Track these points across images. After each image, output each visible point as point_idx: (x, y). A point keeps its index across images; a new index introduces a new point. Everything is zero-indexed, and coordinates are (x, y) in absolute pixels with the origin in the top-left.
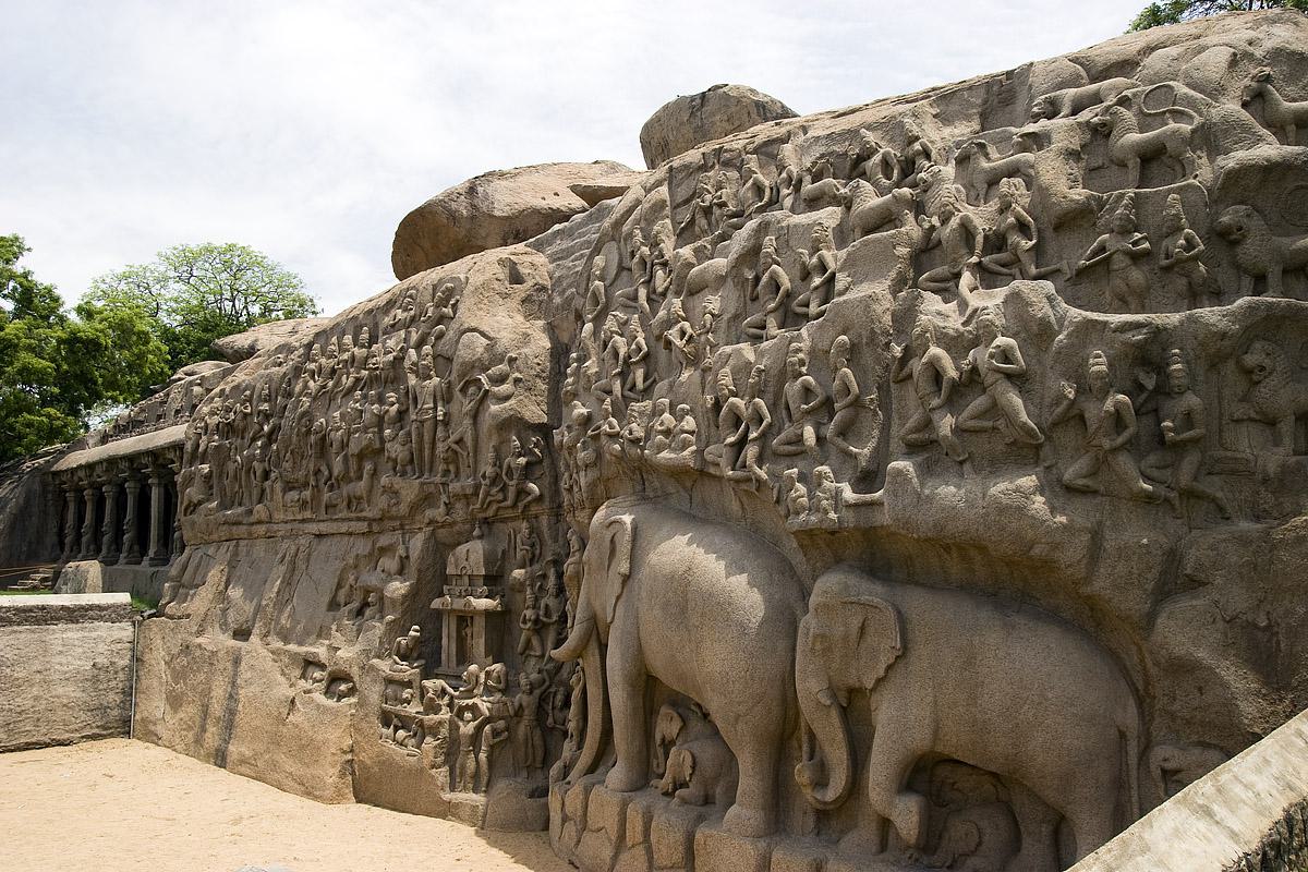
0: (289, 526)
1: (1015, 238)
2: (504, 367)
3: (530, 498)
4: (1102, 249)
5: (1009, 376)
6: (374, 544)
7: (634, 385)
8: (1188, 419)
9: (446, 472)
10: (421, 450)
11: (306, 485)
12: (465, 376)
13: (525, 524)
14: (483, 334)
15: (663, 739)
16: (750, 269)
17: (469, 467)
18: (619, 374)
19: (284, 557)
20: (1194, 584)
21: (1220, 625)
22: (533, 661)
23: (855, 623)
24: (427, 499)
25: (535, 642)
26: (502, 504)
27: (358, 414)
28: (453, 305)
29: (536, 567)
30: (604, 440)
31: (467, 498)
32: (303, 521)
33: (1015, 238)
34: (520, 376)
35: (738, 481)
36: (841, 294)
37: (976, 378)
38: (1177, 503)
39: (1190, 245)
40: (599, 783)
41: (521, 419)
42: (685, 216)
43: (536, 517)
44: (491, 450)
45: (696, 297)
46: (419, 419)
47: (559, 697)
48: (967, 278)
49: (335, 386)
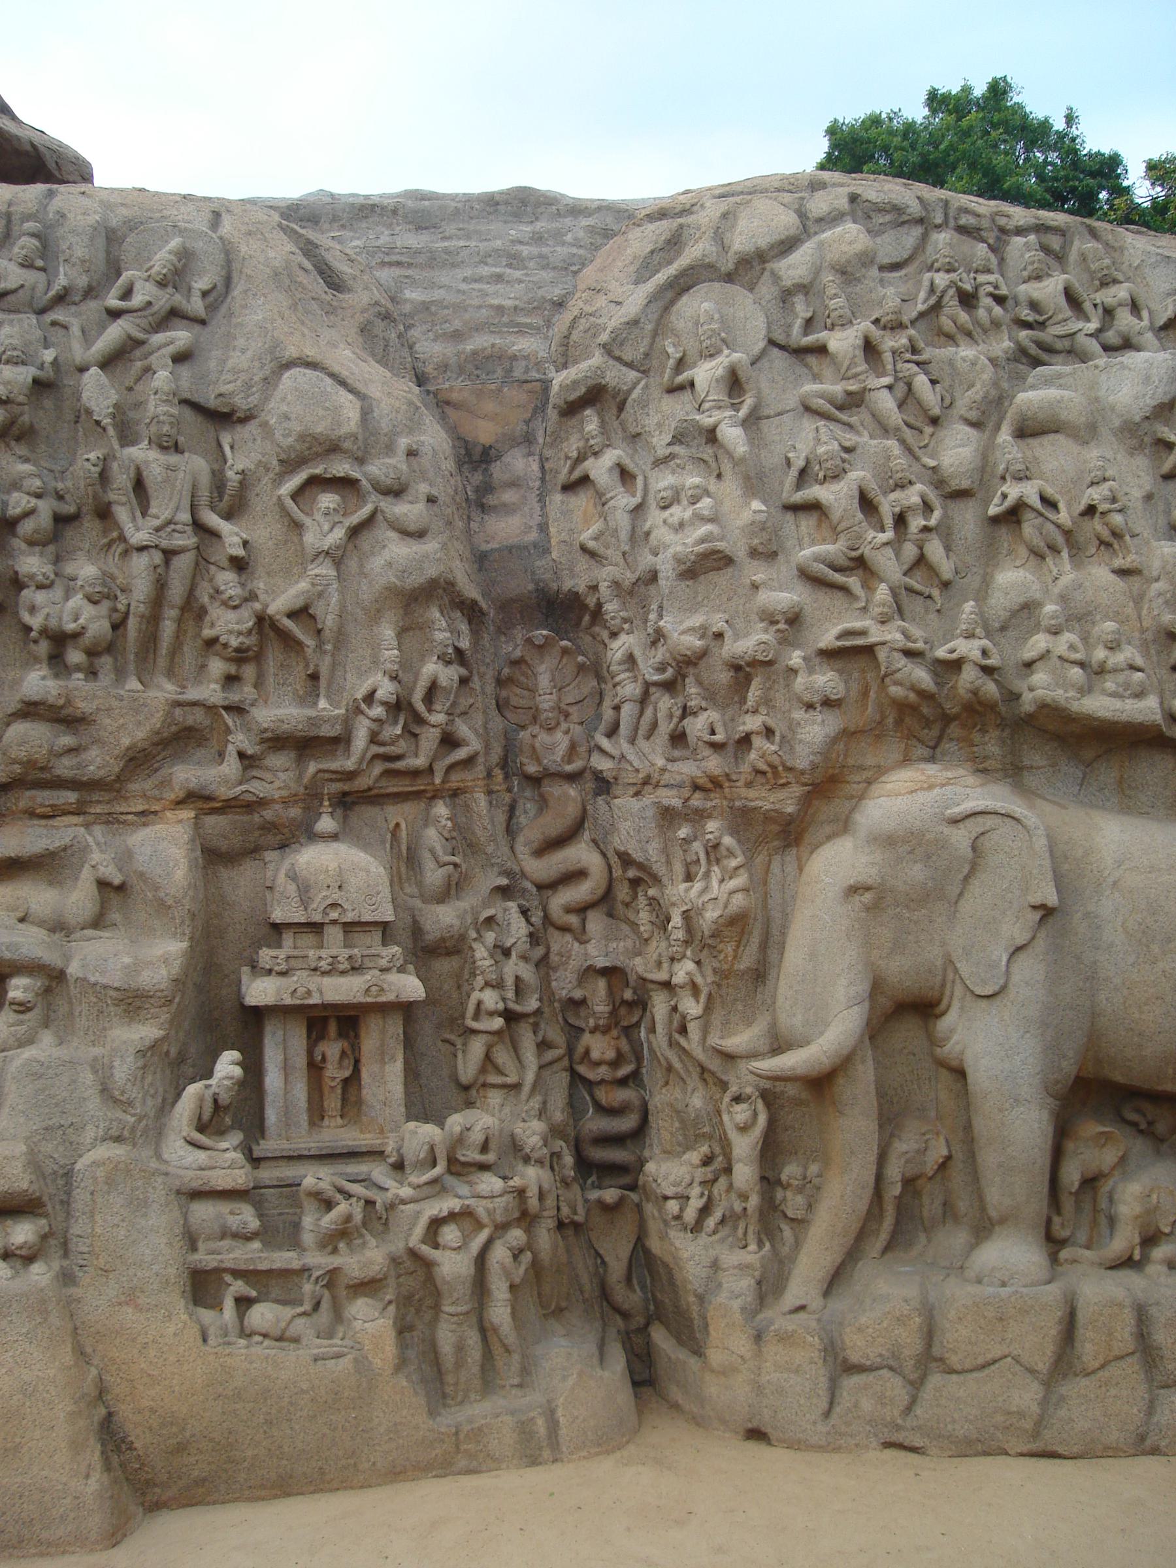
3: (462, 753)
9: (231, 680)
10: (154, 619)
13: (441, 810)
14: (343, 383)
16: (1171, 430)
17: (314, 677)
24: (181, 737)
28: (205, 294)
31: (304, 744)
34: (435, 492)
41: (452, 584)
43: (455, 793)
45: (1030, 441)
46: (164, 544)
47: (569, 1160)
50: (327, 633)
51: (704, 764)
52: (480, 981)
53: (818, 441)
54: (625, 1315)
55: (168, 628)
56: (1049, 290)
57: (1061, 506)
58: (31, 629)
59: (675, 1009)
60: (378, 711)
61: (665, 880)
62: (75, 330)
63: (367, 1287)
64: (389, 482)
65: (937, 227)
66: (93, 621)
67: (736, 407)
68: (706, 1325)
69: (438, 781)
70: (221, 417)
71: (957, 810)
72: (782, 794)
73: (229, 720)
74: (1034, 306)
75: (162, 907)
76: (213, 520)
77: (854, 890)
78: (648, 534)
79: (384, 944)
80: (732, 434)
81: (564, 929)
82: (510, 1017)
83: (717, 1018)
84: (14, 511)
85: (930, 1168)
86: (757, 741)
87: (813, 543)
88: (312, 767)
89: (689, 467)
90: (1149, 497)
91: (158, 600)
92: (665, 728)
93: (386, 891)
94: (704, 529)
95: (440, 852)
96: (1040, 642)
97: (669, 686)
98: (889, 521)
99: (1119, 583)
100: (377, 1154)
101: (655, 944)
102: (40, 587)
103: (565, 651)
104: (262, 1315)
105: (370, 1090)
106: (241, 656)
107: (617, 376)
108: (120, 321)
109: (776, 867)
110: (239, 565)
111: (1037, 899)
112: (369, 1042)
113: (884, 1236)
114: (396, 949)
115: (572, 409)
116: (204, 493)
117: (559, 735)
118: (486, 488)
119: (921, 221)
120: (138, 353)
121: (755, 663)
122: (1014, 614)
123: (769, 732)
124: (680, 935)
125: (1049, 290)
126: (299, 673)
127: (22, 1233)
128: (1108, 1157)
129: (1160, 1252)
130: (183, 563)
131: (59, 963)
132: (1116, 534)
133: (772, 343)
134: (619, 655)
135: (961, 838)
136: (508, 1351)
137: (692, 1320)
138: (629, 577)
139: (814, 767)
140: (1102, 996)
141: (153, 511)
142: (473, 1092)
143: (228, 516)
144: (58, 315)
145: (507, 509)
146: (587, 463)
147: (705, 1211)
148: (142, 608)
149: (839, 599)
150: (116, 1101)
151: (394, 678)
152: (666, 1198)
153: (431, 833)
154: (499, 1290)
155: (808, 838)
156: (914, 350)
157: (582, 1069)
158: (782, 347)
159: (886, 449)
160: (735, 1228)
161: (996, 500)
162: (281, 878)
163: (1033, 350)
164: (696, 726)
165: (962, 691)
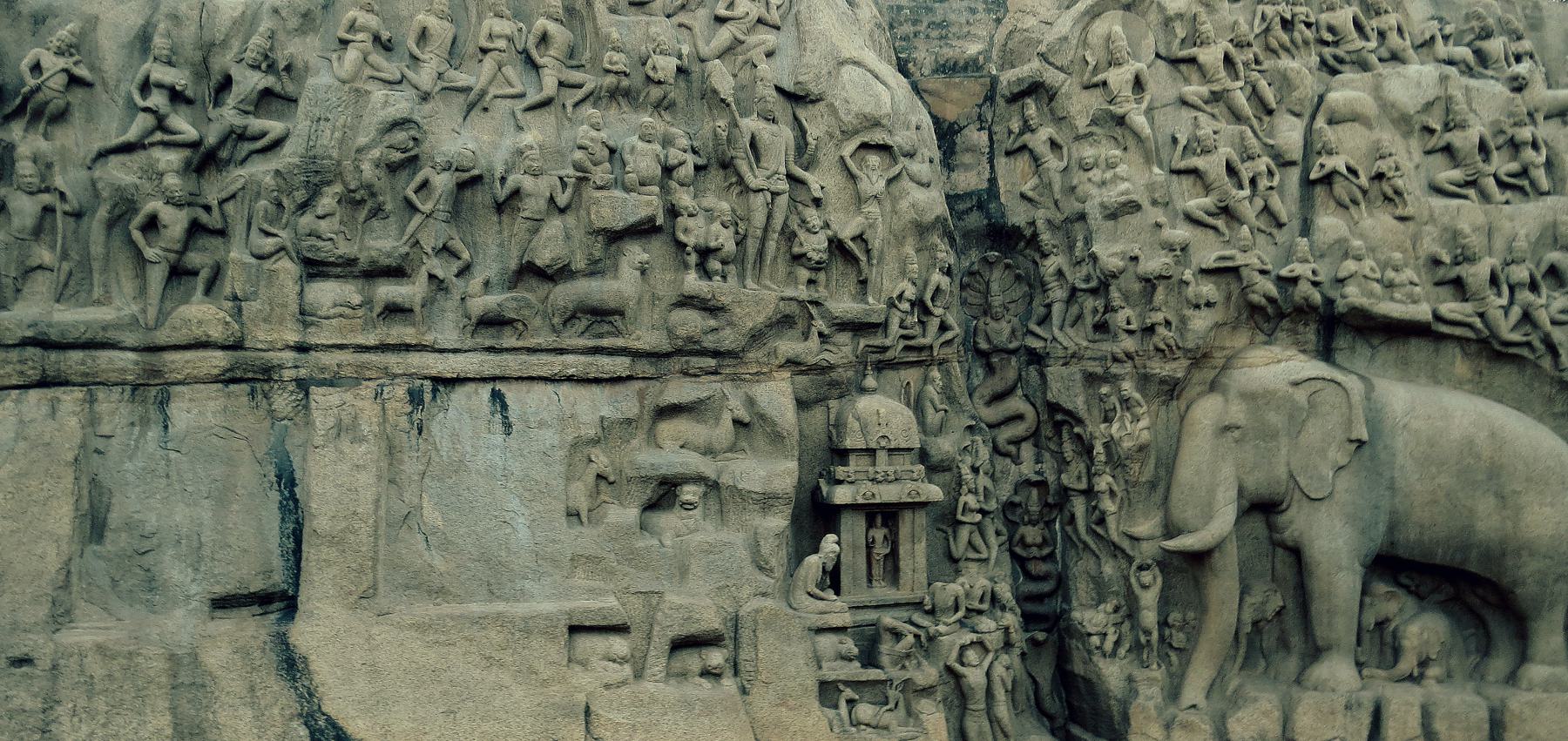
0: (330, 359)
3: (949, 335)
6: (641, 395)
9: (811, 282)
10: (764, 240)
11: (397, 272)
12: (856, 132)
17: (864, 283)
19: (339, 429)
24: (784, 322)
25: (978, 541)
27: (606, 152)
31: (858, 328)
32: (383, 348)
46: (773, 188)
47: (1018, 611)
49: (490, 83)
50: (875, 253)
51: (1123, 344)
53: (1197, 126)
54: (1051, 718)
55: (771, 246)
56: (1343, 17)
57: (1361, 173)
58: (685, 245)
59: (1095, 508)
60: (906, 306)
61: (1087, 422)
62: (697, 30)
63: (927, 691)
64: (907, 148)
66: (725, 239)
67: (1139, 101)
68: (1126, 719)
70: (796, 98)
72: (1174, 365)
73: (813, 310)
74: (1331, 29)
75: (777, 438)
76: (798, 172)
77: (1227, 428)
78: (1073, 189)
80: (1139, 120)
81: (1006, 455)
82: (981, 511)
84: (672, 161)
85: (1270, 614)
86: (1161, 330)
87: (1191, 197)
88: (863, 343)
89: (1104, 142)
90: (1417, 167)
91: (766, 230)
92: (1089, 320)
93: (915, 427)
94: (1124, 186)
95: (937, 402)
96: (1350, 266)
97: (1093, 292)
98: (1246, 182)
99: (1400, 226)
100: (918, 605)
101: (1073, 464)
102: (691, 215)
103: (1008, 266)
104: (865, 711)
105: (905, 564)
106: (818, 267)
107: (1052, 77)
108: (728, 25)
109: (1163, 413)
110: (817, 202)
111: (1354, 437)
112: (904, 530)
113: (1240, 660)
115: (1016, 98)
116: (792, 152)
117: (1004, 324)
120: (739, 49)
121: (1161, 277)
122: (1331, 246)
123: (1168, 323)
124: (1103, 458)
125: (1343, 17)
126: (853, 278)
127: (716, 657)
128: (1389, 608)
130: (783, 200)
131: (713, 477)
132: (1397, 192)
133: (1158, 55)
134: (1051, 270)
135: (1301, 395)
136: (1006, 736)
137: (1111, 718)
138: (1058, 217)
141: (763, 164)
142: (961, 564)
143: (806, 169)
144: (682, 18)
145: (967, 167)
146: (1027, 137)
147: (1117, 643)
148: (759, 233)
149: (1211, 232)
150: (761, 568)
152: (1090, 635)
153: (930, 388)
154: (1000, 694)
155: (1185, 394)
156: (1257, 62)
157: (1018, 550)
159: (1241, 133)
160: (1140, 654)
161: (1316, 168)
162: (851, 419)
163: (1331, 62)
164: (1120, 318)
165: (1297, 298)
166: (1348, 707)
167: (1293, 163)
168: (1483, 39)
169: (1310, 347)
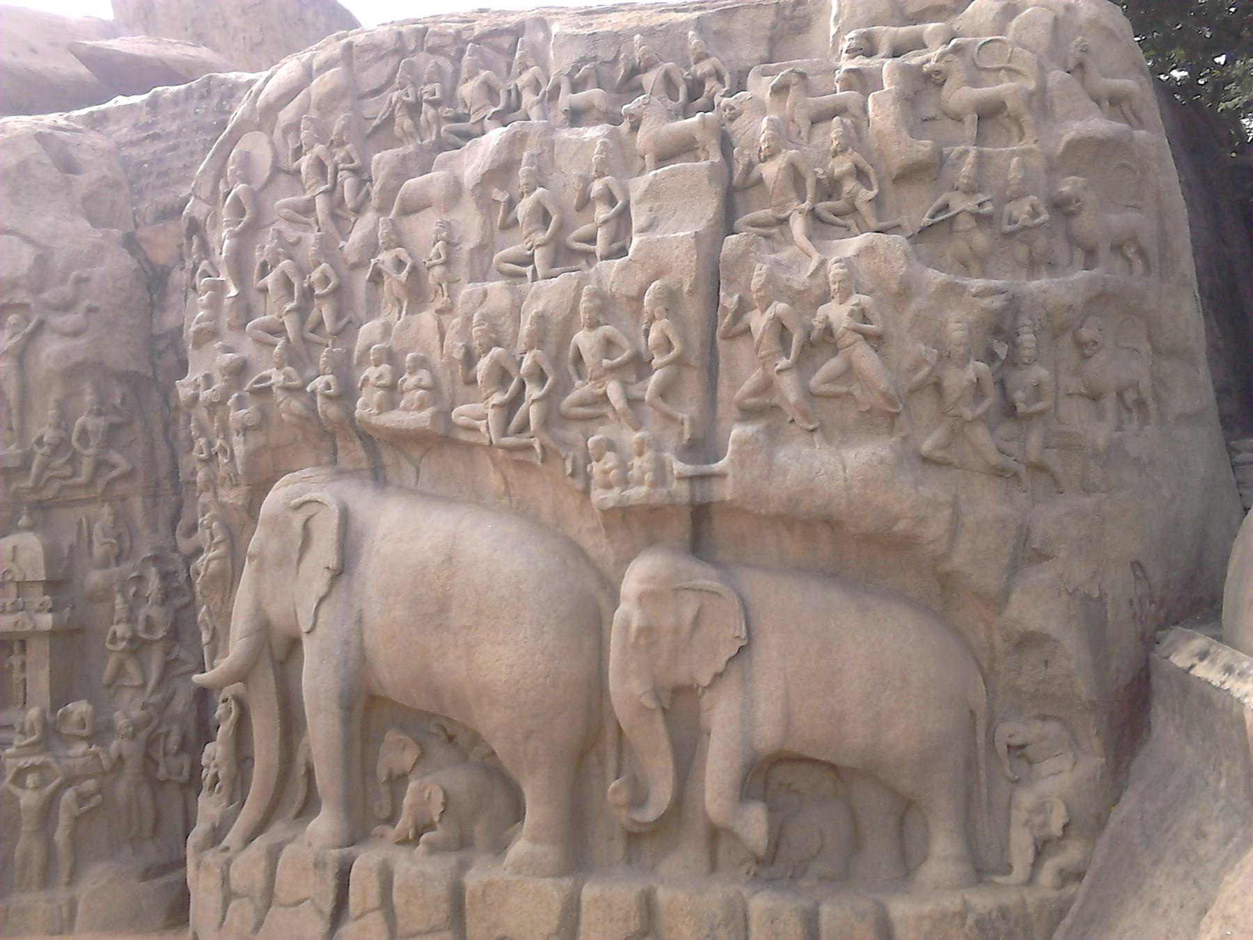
1: (849, 186)
2: (67, 289)
3: (115, 473)
4: (946, 207)
5: (867, 336)
7: (321, 322)
8: (1037, 391)
13: (106, 510)
15: (390, 776)
16: (502, 189)
17: (10, 429)
18: (296, 310)
20: (1041, 557)
21: (1064, 597)
22: (127, 695)
23: (689, 612)
25: (131, 667)
26: (69, 482)
29: (126, 566)
30: (279, 396)
33: (849, 186)
35: (510, 449)
36: (642, 231)
37: (828, 339)
38: (1023, 475)
39: (1035, 213)
40: (289, 841)
42: (375, 110)
43: (124, 499)
44: (51, 403)
47: (174, 739)
48: (798, 226)
52: (115, 620)
65: (414, 52)
69: (99, 490)
71: (297, 501)
77: (252, 557)
79: (45, 594)
83: (221, 644)
88: (14, 487)
100: (10, 727)
114: (47, 597)
118: (164, 295)
119: (396, 52)
129: (423, 837)
133: (276, 170)
135: (297, 520)
139: (246, 473)
140: (367, 635)
142: (112, 691)
147: (216, 778)
151: (58, 426)
154: (64, 819)
158: (288, 172)
166: (316, 865)
167: (355, 267)
168: (646, 70)
169: (364, 464)
